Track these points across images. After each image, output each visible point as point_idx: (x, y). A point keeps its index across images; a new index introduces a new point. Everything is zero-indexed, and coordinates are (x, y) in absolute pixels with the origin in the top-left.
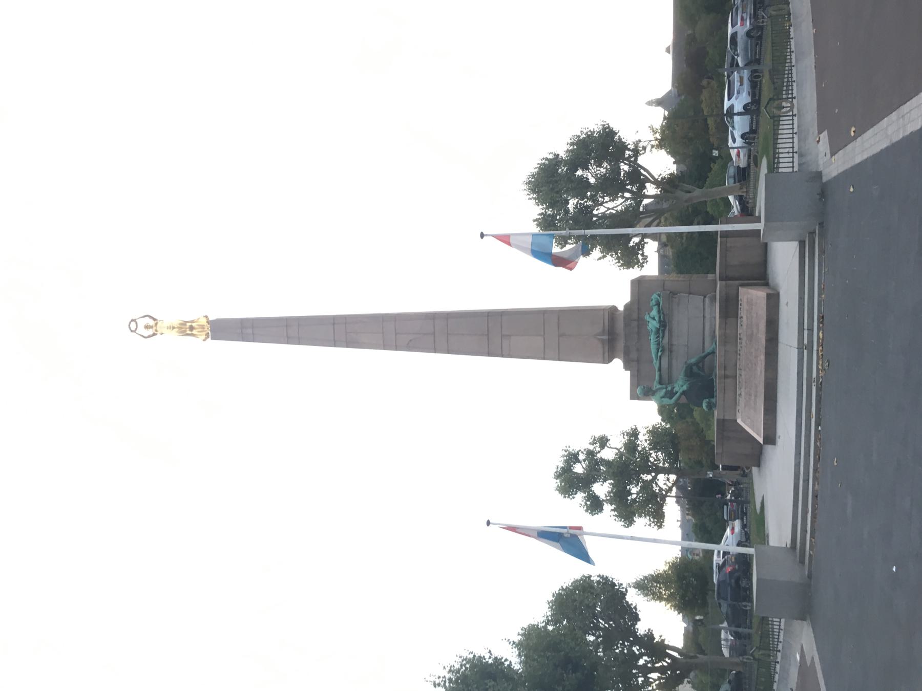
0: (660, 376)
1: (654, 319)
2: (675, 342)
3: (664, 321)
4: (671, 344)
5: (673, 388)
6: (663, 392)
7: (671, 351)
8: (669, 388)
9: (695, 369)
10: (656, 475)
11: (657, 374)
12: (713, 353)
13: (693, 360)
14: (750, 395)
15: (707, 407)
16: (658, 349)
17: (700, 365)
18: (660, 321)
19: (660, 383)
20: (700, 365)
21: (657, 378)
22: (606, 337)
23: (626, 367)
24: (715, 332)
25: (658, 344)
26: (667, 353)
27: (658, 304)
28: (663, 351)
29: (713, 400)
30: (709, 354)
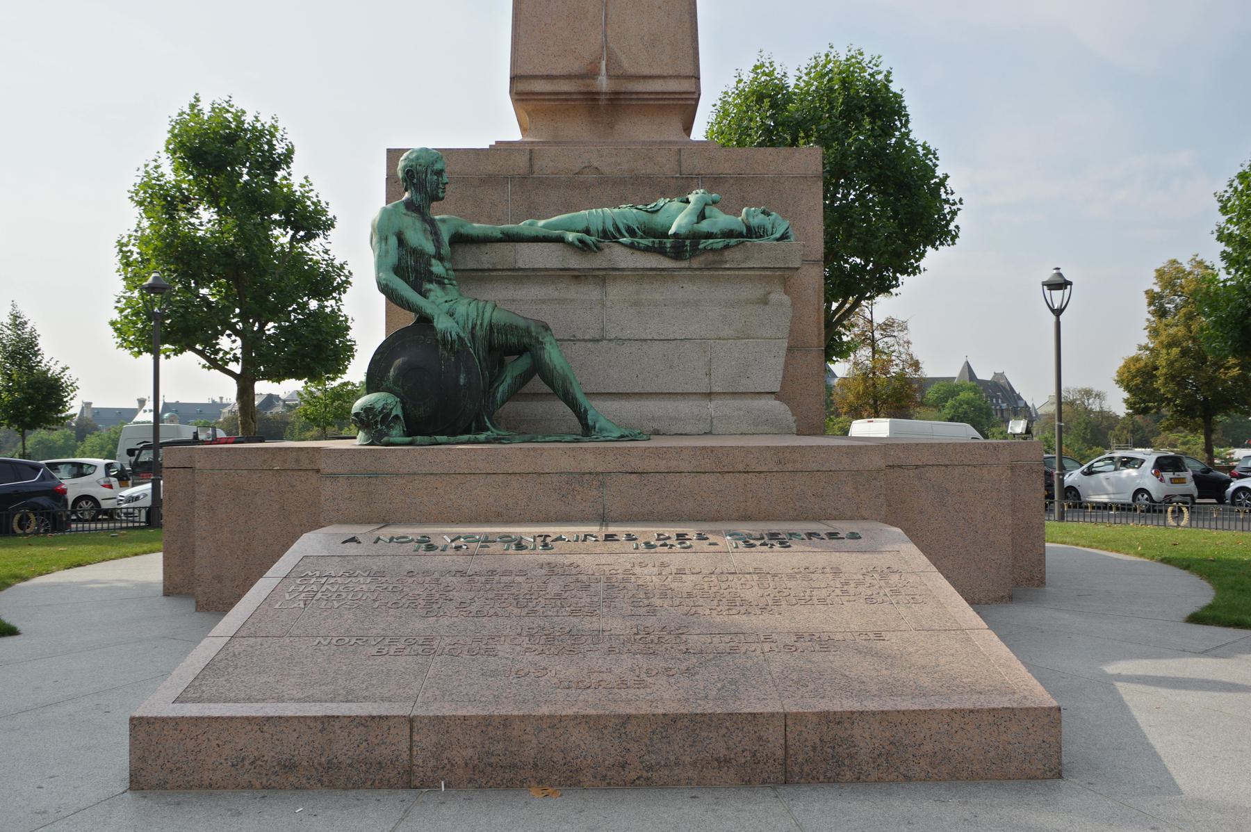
0: (485, 240)
1: (702, 216)
2: (616, 292)
3: (695, 251)
4: (602, 277)
5: (440, 281)
6: (418, 238)
7: (578, 276)
8: (437, 268)
9: (516, 367)
10: (237, 333)
11: (494, 229)
12: (587, 430)
13: (553, 355)
14: (431, 607)
15: (368, 410)
16: (587, 231)
17: (537, 384)
18: (696, 237)
19: (460, 240)
20: (537, 384)
21: (477, 227)
22: (603, 83)
23: (502, 148)
24: (657, 433)
25: (605, 234)
26: (575, 261)
27: (752, 232)
28: (583, 247)
29: (396, 433)
30: (582, 415)
